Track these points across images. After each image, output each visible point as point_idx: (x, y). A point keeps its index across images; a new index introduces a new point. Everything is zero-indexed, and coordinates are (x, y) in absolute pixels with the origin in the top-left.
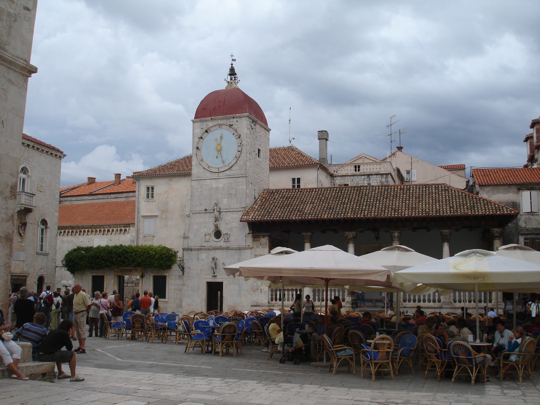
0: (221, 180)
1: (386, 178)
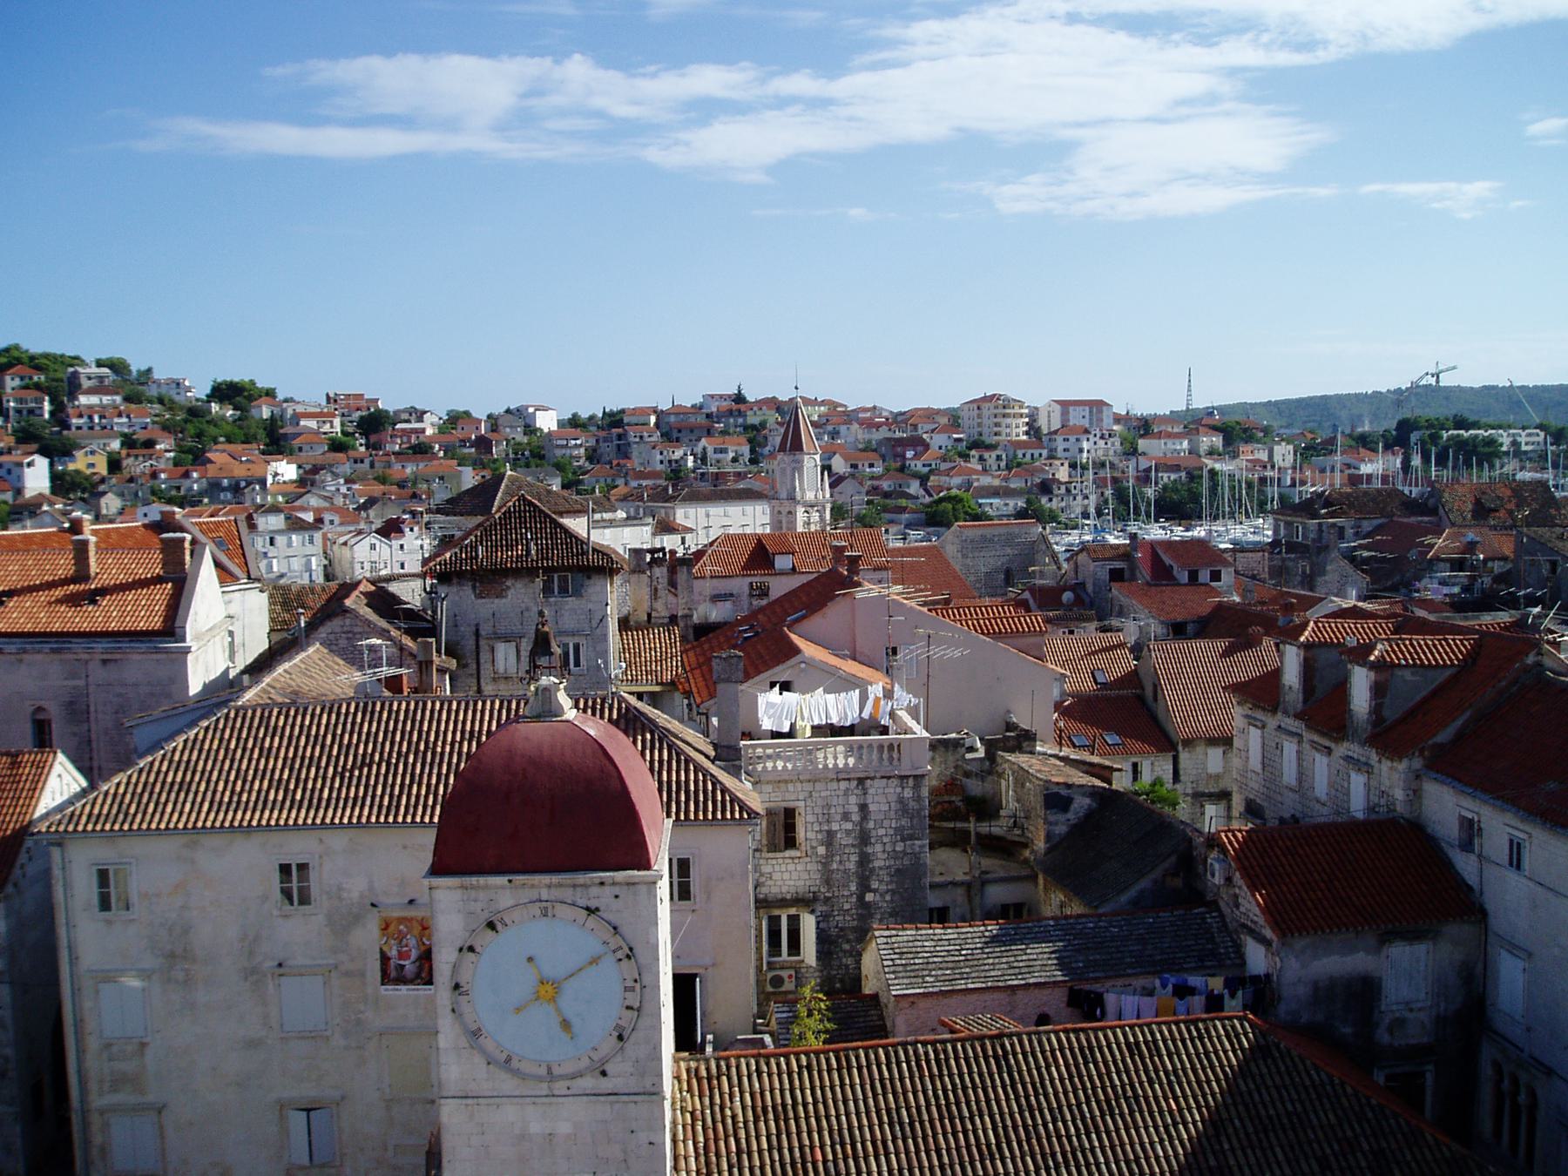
1: (917, 787)
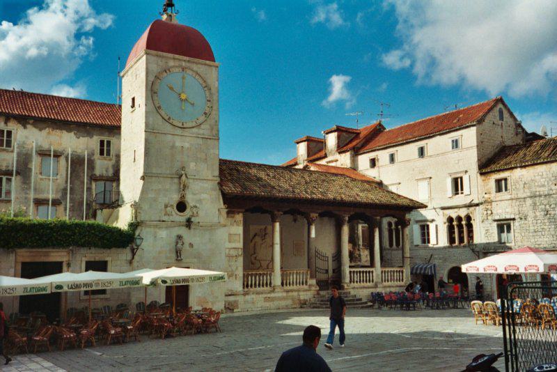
0: (188, 139)
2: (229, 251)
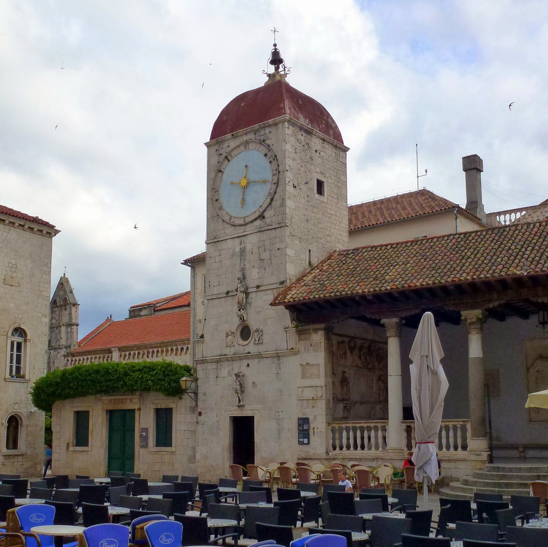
2: (302, 391)
